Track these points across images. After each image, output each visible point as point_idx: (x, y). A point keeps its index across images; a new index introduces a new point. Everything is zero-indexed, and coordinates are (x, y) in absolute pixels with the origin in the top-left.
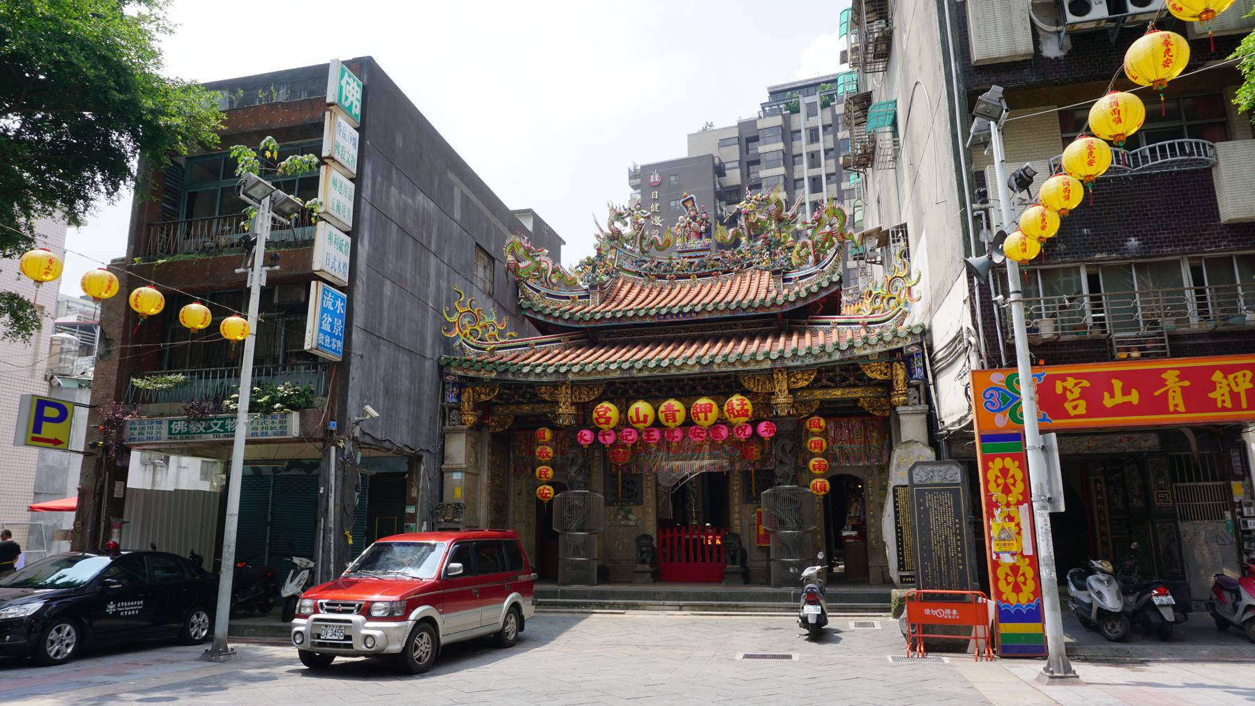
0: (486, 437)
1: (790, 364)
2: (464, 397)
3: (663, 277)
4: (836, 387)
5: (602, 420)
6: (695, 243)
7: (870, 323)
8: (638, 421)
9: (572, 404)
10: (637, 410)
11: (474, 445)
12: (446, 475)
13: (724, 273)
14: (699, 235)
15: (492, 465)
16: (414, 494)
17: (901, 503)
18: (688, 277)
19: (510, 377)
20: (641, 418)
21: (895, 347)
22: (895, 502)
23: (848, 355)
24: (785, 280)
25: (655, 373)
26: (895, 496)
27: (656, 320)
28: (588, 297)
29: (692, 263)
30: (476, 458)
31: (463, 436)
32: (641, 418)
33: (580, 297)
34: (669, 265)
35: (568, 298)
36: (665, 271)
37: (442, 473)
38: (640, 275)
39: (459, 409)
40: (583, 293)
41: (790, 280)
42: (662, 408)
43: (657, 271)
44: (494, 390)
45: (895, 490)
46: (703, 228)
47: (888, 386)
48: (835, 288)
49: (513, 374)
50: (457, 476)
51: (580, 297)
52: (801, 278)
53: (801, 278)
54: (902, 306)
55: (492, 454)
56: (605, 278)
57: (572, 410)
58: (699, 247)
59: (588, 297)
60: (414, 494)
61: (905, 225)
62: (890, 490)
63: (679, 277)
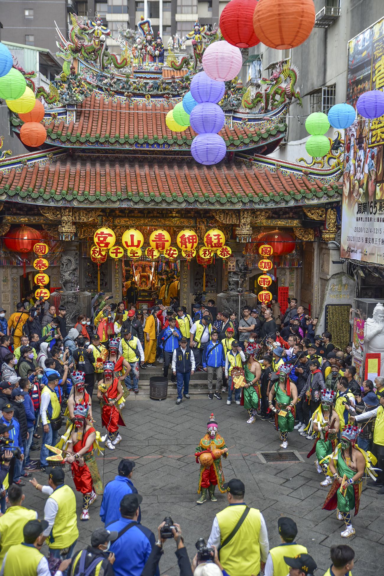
1: (257, 206)
3: (122, 94)
6: (149, 66)
7: (311, 173)
8: (132, 245)
9: (74, 223)
10: (132, 236)
13: (174, 96)
14: (153, 58)
17: (330, 316)
18: (143, 96)
19: (20, 200)
20: (136, 243)
21: (335, 200)
22: (326, 316)
23: (300, 204)
24: (234, 118)
25: (150, 206)
26: (326, 312)
27: (134, 148)
28: (65, 113)
29: (147, 83)
32: (136, 243)
33: (59, 114)
34: (127, 82)
35: (49, 115)
36: (123, 88)
38: (101, 89)
40: (61, 110)
41: (240, 119)
42: (153, 237)
43: (115, 88)
45: (327, 308)
46: (157, 53)
47: (323, 223)
48: (280, 137)
49: (23, 198)
51: (59, 114)
52: (250, 120)
53: (250, 120)
54: (341, 167)
56: (81, 98)
57: (73, 229)
58: (153, 69)
59: (65, 113)
61: (334, 86)
62: (324, 307)
63: (135, 95)
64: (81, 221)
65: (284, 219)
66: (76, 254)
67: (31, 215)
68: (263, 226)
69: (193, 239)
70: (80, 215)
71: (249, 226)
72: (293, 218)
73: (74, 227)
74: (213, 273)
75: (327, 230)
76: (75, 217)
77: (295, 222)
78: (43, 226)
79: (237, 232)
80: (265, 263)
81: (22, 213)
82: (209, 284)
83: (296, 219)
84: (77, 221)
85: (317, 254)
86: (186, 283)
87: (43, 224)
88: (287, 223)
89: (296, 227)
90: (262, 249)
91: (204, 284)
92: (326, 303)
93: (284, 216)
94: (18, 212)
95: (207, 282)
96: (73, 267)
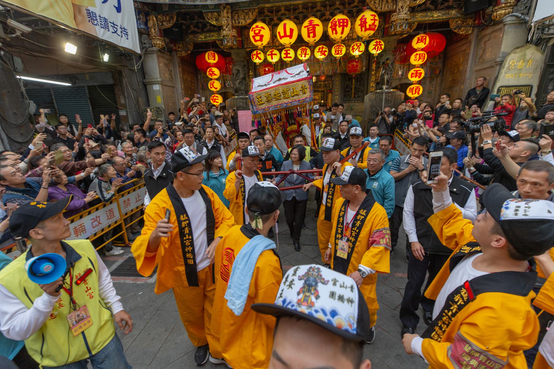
0: (177, 61)
2: (150, 24)
4: (436, 9)
5: (258, 38)
9: (233, 27)
11: (167, 65)
12: (148, 87)
15: (184, 81)
16: (123, 101)
30: (170, 74)
31: (155, 56)
37: (145, 86)
39: (149, 35)
44: (172, 18)
50: (157, 87)
55: (183, 72)
57: (234, 33)
60: (123, 101)
64: (240, 25)
65: (442, 9)
66: (245, 66)
67: (207, 32)
68: (417, 21)
69: (343, 22)
70: (238, 17)
71: (407, 9)
72: (449, 8)
73: (234, 30)
74: (360, 85)
75: (502, 4)
76: (235, 22)
77: (454, 12)
78: (217, 42)
79: (393, 19)
80: (420, 54)
81: (199, 31)
82: (356, 95)
83: (455, 8)
84: (237, 25)
85: (475, 46)
86: (337, 95)
87: (216, 40)
88: (444, 15)
89: (453, 19)
90: (418, 38)
91: (353, 95)
92: (498, 85)
93: (442, 7)
94: (196, 29)
95: (355, 94)
96: (241, 76)
